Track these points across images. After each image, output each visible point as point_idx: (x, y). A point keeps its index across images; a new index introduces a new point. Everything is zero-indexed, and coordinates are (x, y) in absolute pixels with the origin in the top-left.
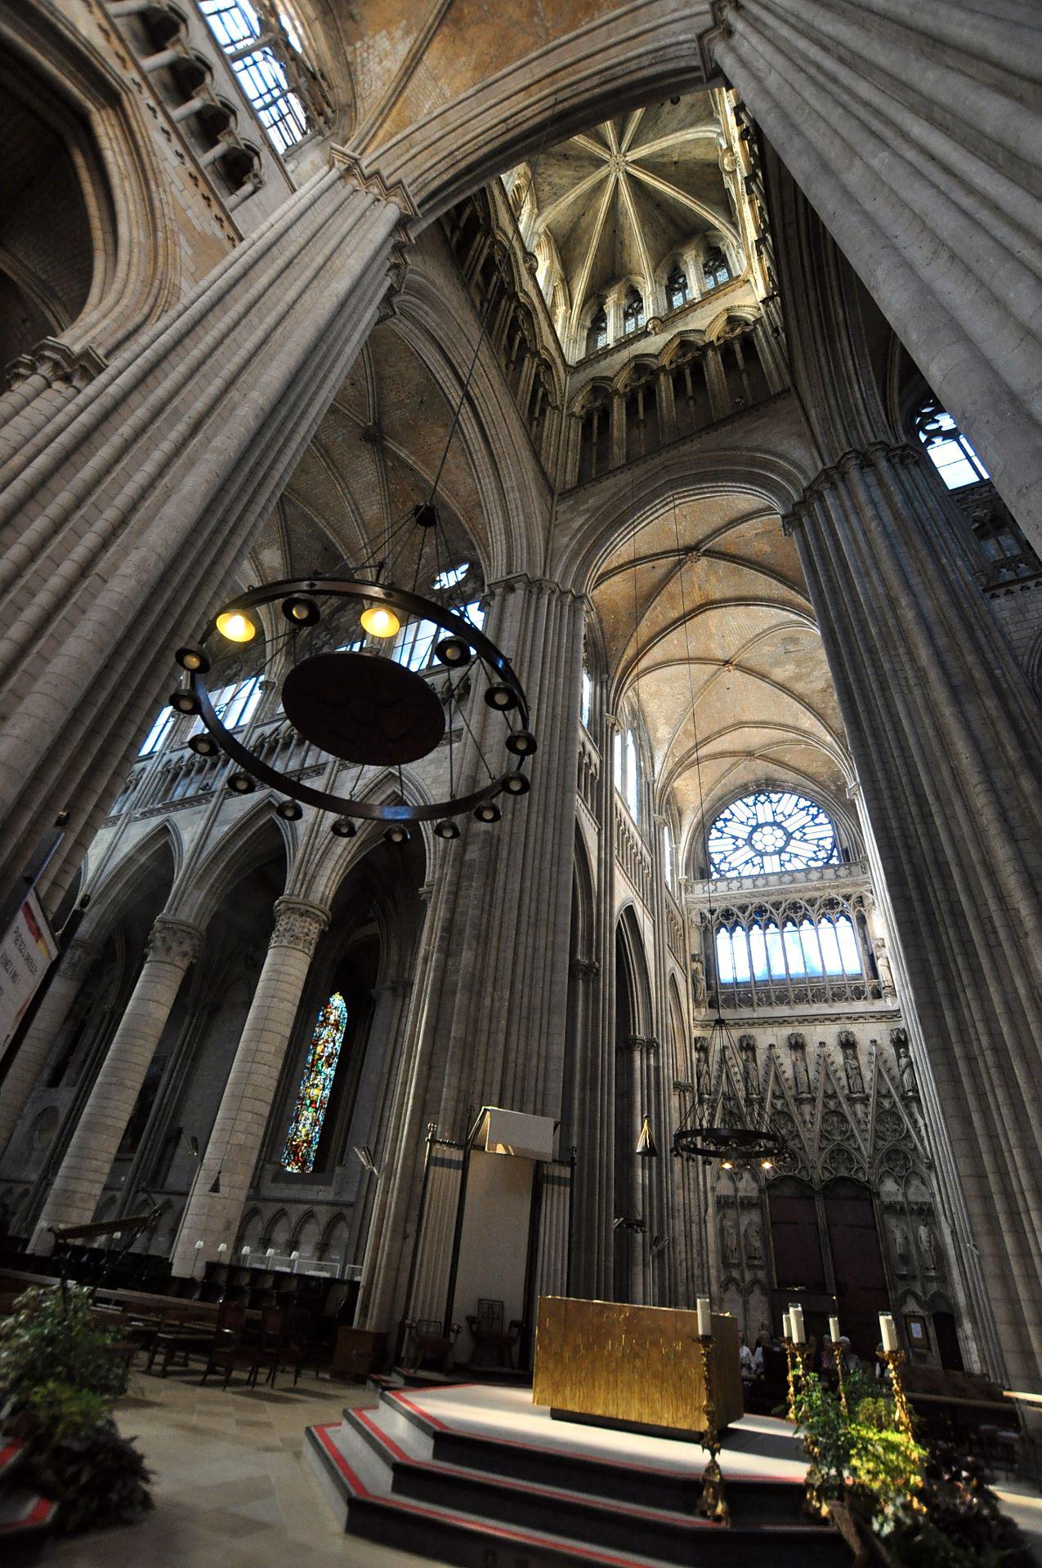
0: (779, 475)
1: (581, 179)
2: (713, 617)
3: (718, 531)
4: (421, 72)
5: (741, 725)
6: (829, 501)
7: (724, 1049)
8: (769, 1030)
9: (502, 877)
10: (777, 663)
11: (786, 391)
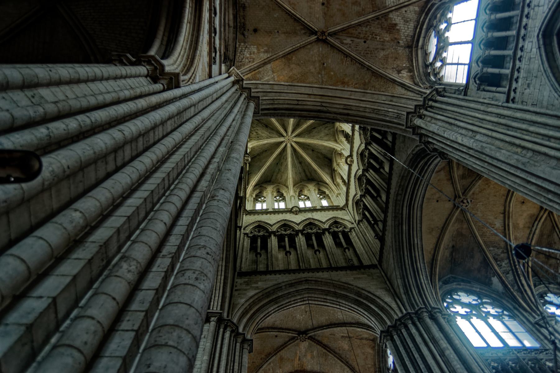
0: (376, 307)
1: (271, 137)
3: (321, 327)
4: (269, 66)
6: (413, 331)
11: (373, 266)
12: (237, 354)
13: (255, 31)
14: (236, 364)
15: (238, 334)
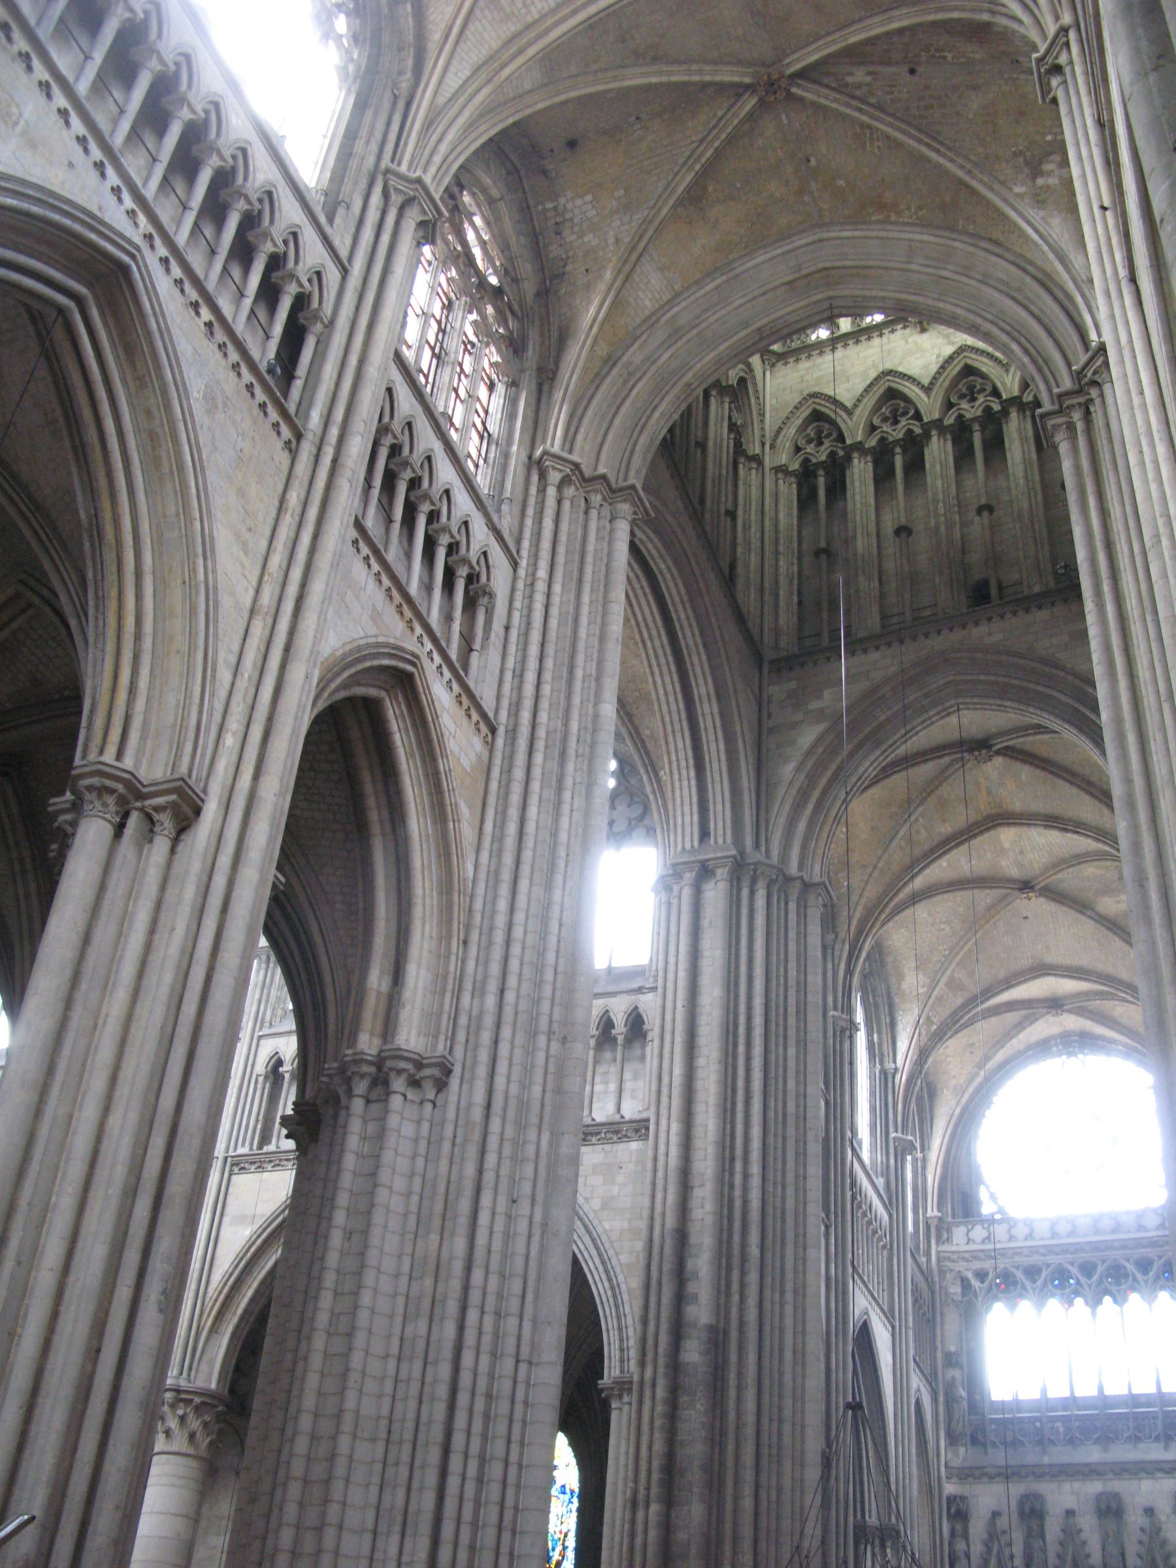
2: (1007, 835)
5: (1042, 969)
7: (995, 1514)
8: (1067, 1487)
9: (732, 1393)
10: (1107, 890)
12: (792, 934)
13: (572, 144)
14: (792, 965)
15: (788, 879)
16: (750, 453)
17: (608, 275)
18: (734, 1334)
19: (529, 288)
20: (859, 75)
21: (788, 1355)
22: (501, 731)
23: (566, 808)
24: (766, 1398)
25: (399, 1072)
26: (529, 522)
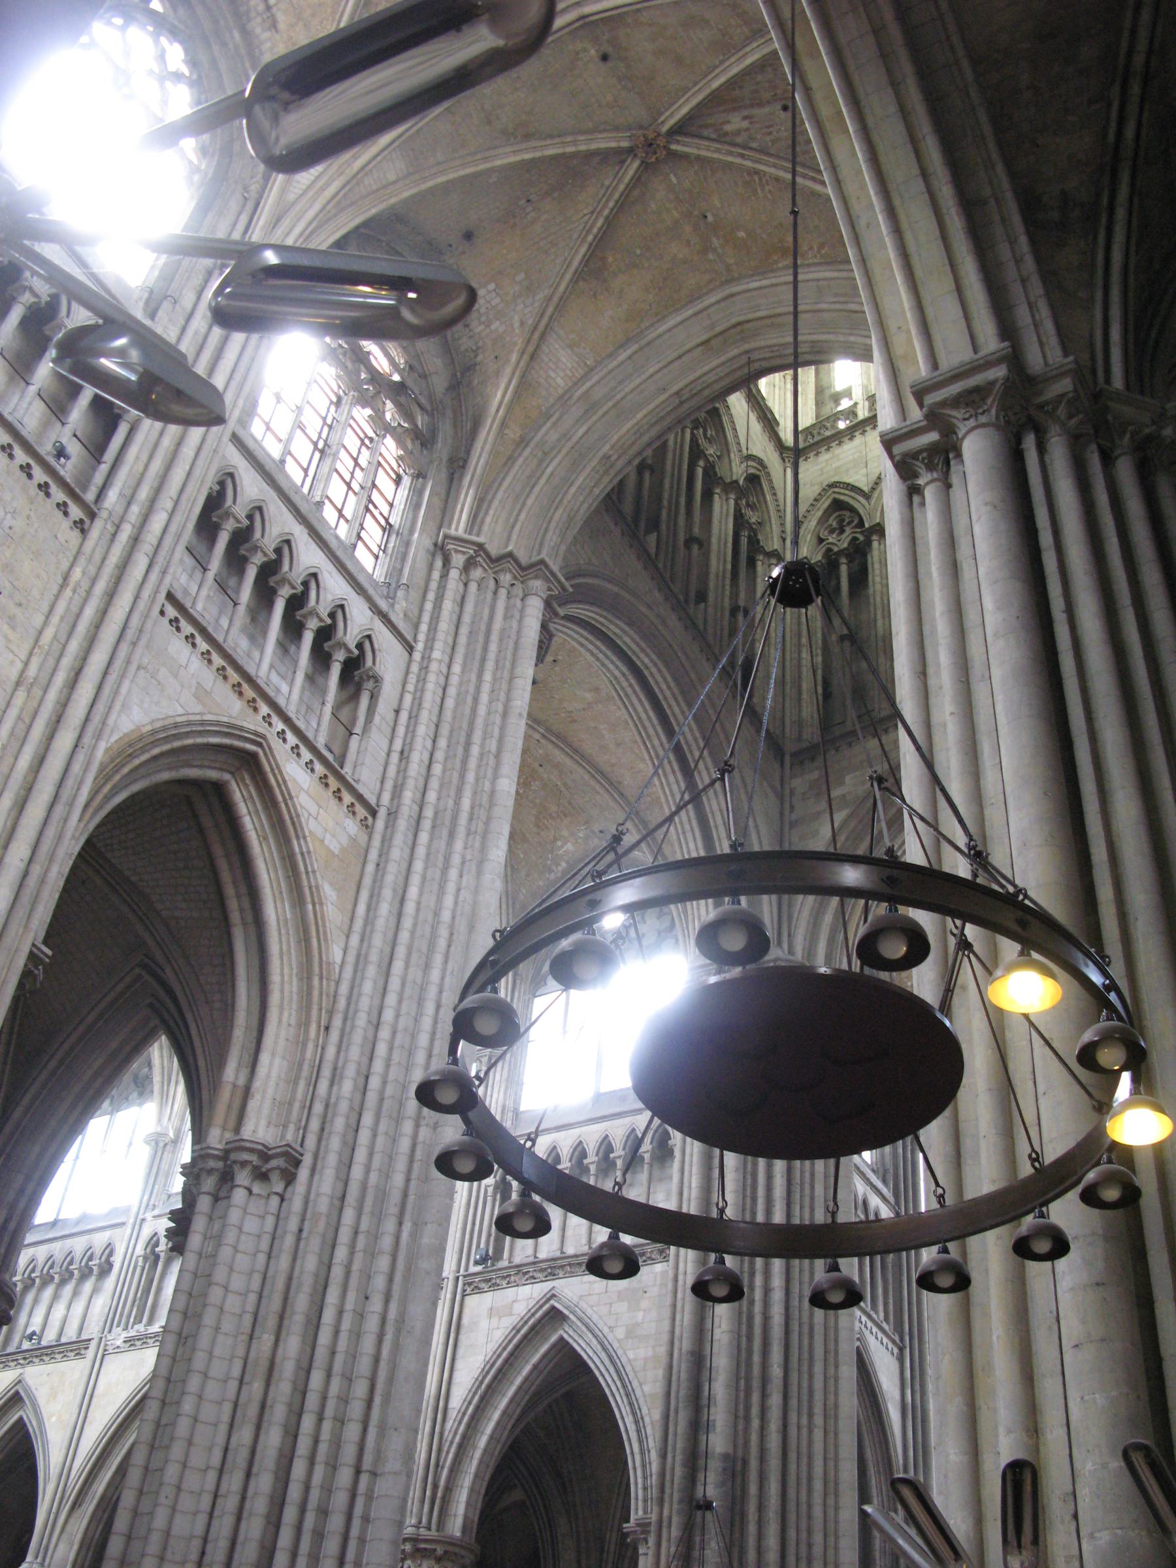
9: (752, 1528)
13: (469, 236)
16: (768, 549)
17: (514, 357)
18: (754, 1464)
19: (440, 383)
20: (735, 122)
21: (818, 1485)
22: (382, 813)
23: (451, 887)
24: (792, 1534)
25: (244, 1164)
26: (429, 606)
